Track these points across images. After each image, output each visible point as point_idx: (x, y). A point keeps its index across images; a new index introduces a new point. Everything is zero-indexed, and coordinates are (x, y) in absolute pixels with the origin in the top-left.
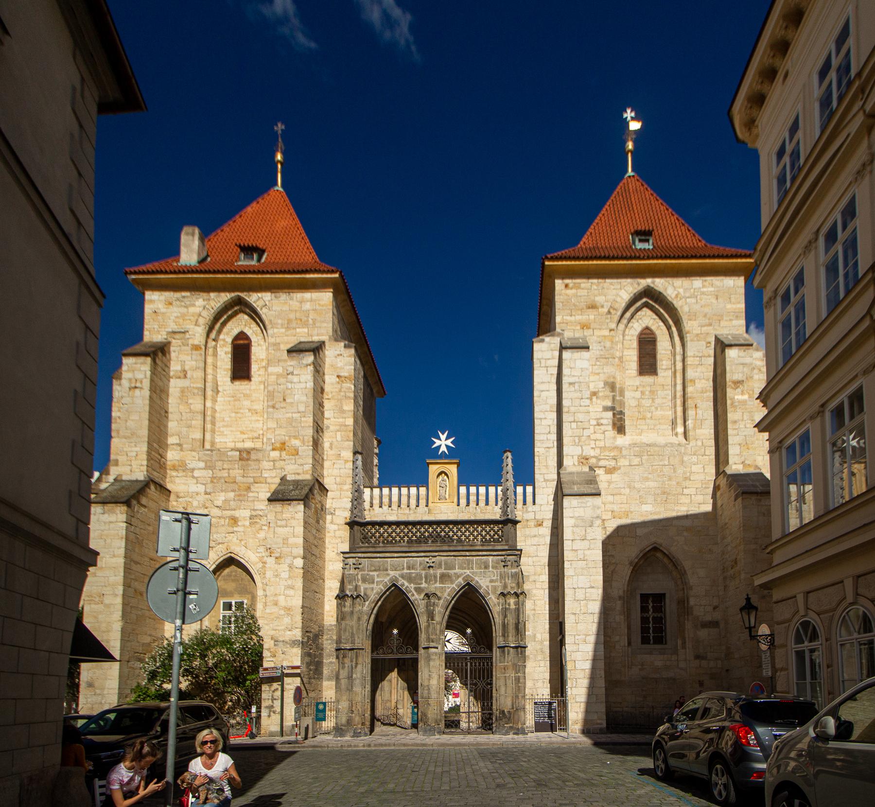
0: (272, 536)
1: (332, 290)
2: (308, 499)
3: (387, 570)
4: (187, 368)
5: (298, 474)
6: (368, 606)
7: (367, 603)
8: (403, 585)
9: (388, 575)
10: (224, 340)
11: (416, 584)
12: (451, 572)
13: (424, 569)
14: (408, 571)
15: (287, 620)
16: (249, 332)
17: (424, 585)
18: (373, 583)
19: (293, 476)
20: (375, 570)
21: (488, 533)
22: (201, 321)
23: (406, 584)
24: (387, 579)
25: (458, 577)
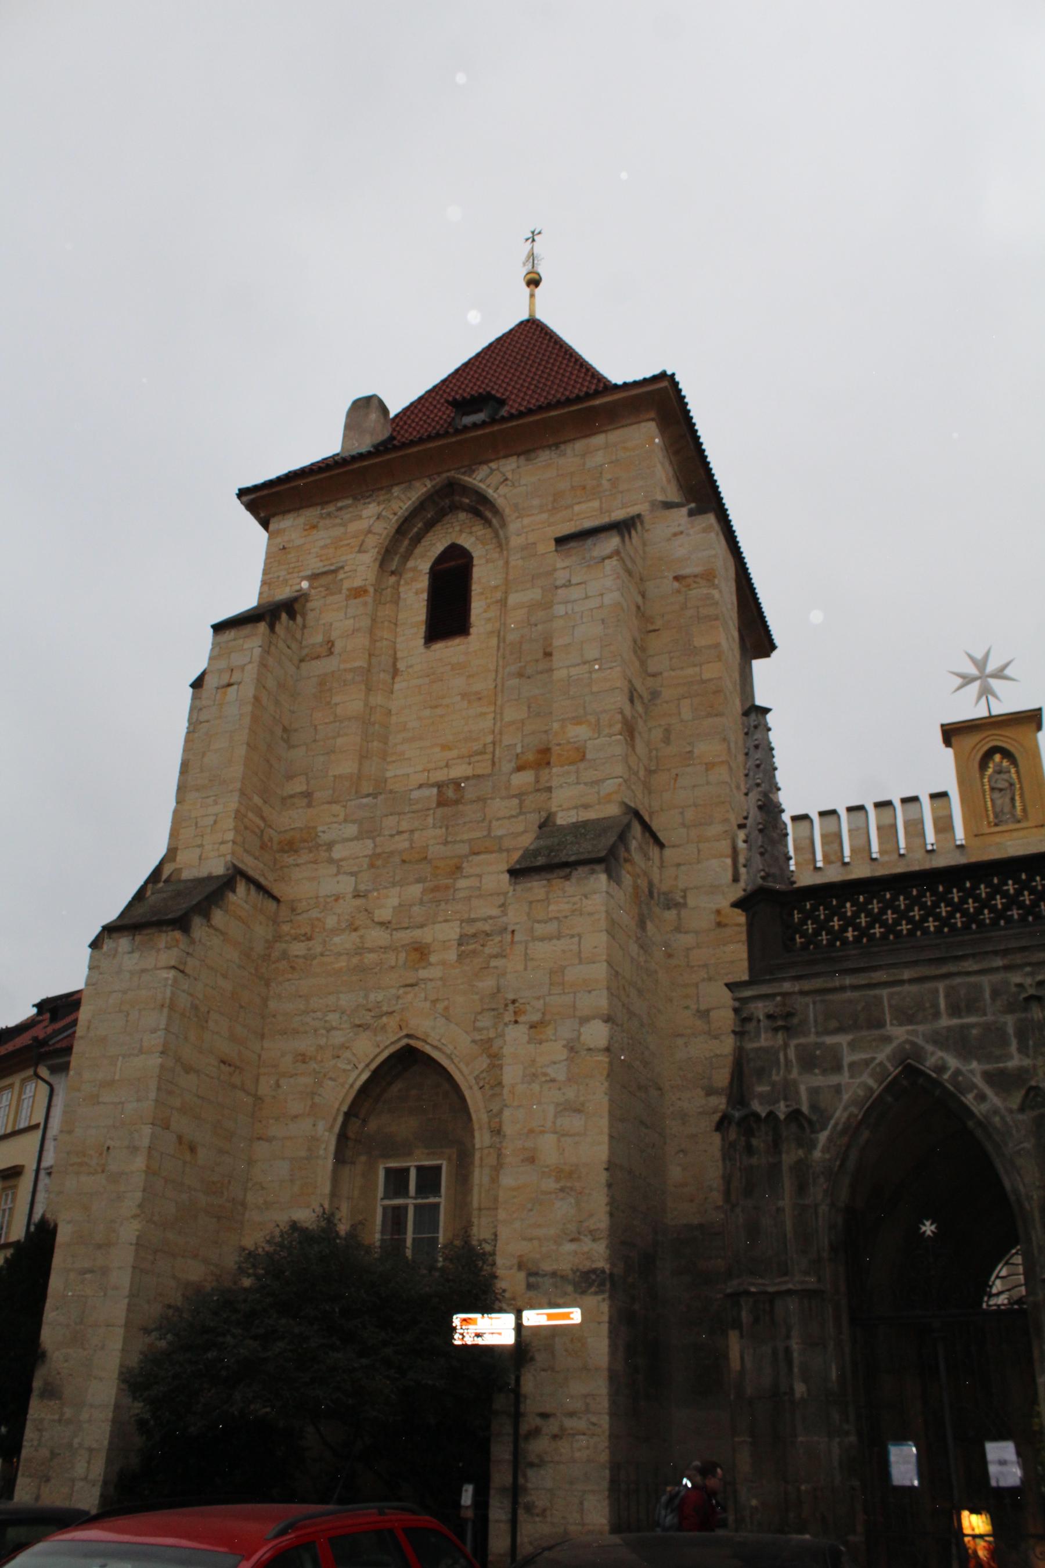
0: (521, 967)
1: (652, 415)
2: (617, 859)
3: (881, 1024)
4: (334, 635)
5: (586, 807)
6: (826, 1149)
7: (823, 1137)
8: (941, 1068)
9: (888, 1039)
10: (414, 569)
13: (1010, 1009)
14: (955, 1021)
15: (563, 1209)
16: (466, 541)
17: (1015, 1061)
18: (837, 1068)
19: (573, 812)
20: (840, 1030)
22: (371, 541)
23: (953, 1062)
24: (883, 1055)
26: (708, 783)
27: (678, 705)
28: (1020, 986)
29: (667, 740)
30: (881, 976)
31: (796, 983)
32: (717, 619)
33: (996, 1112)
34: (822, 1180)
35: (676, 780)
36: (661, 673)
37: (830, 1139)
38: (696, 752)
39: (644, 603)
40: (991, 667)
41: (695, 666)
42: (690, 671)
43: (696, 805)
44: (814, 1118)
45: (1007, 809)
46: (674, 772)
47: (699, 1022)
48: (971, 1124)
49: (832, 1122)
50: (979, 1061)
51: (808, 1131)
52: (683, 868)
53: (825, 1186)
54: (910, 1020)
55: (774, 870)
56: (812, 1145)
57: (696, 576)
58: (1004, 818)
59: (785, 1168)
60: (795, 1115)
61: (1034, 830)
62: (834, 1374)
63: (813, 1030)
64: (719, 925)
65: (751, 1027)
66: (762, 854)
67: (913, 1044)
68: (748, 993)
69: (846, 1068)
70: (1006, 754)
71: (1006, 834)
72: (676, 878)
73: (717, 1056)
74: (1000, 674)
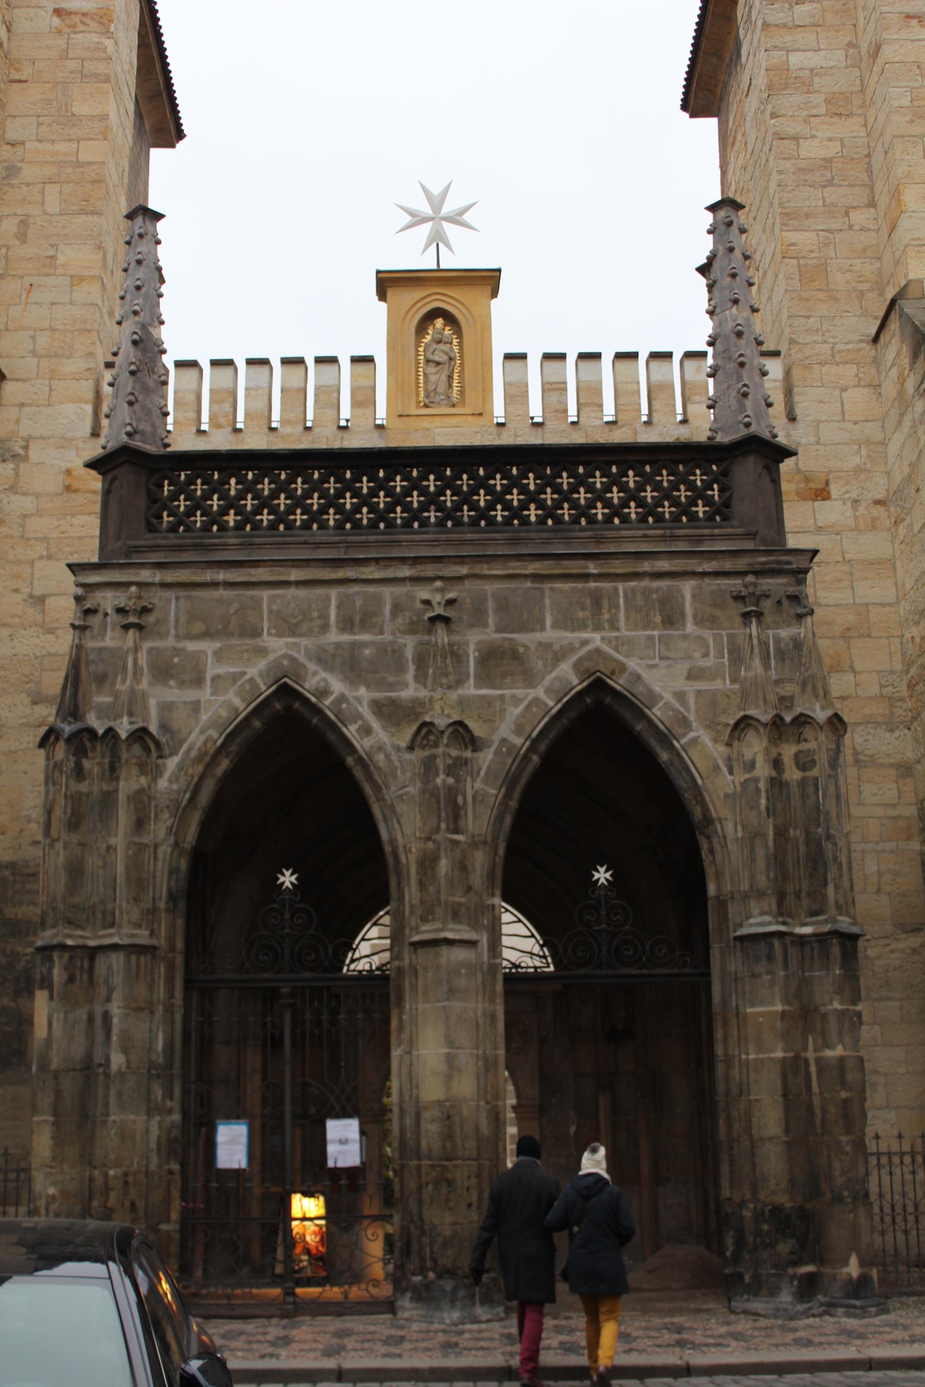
3: (256, 633)
6: (175, 778)
7: (172, 763)
8: (323, 693)
9: (262, 651)
11: (381, 685)
12: (527, 639)
13: (412, 629)
14: (346, 638)
17: (410, 691)
18: (198, 681)
20: (206, 635)
21: (667, 496)
23: (337, 686)
25: (558, 658)
26: (71, 303)
27: (43, 192)
28: (427, 602)
29: (22, 236)
30: (261, 574)
31: (157, 572)
32: (107, 80)
33: (380, 749)
34: (166, 815)
35: (29, 292)
36: (23, 143)
37: (180, 767)
38: (61, 259)
39: (9, 39)
40: (446, 209)
41: (70, 140)
42: (63, 147)
43: (52, 329)
44: (163, 740)
45: (442, 388)
46: (28, 280)
47: (30, 611)
48: (350, 760)
49: (185, 746)
50: (368, 687)
51: (154, 754)
52: (27, 409)
53: (169, 823)
54: (293, 630)
55: (144, 426)
56: (158, 773)
57: (84, 15)
58: (437, 399)
59: (122, 796)
60: (141, 735)
61: (470, 418)
62: (160, 1045)
63: (172, 632)
64: (68, 489)
65: (95, 621)
66: (131, 404)
67: (293, 660)
68: (94, 578)
69: (208, 682)
70: (450, 319)
71: (437, 419)
72: (18, 421)
73: (49, 654)
74: (456, 219)
